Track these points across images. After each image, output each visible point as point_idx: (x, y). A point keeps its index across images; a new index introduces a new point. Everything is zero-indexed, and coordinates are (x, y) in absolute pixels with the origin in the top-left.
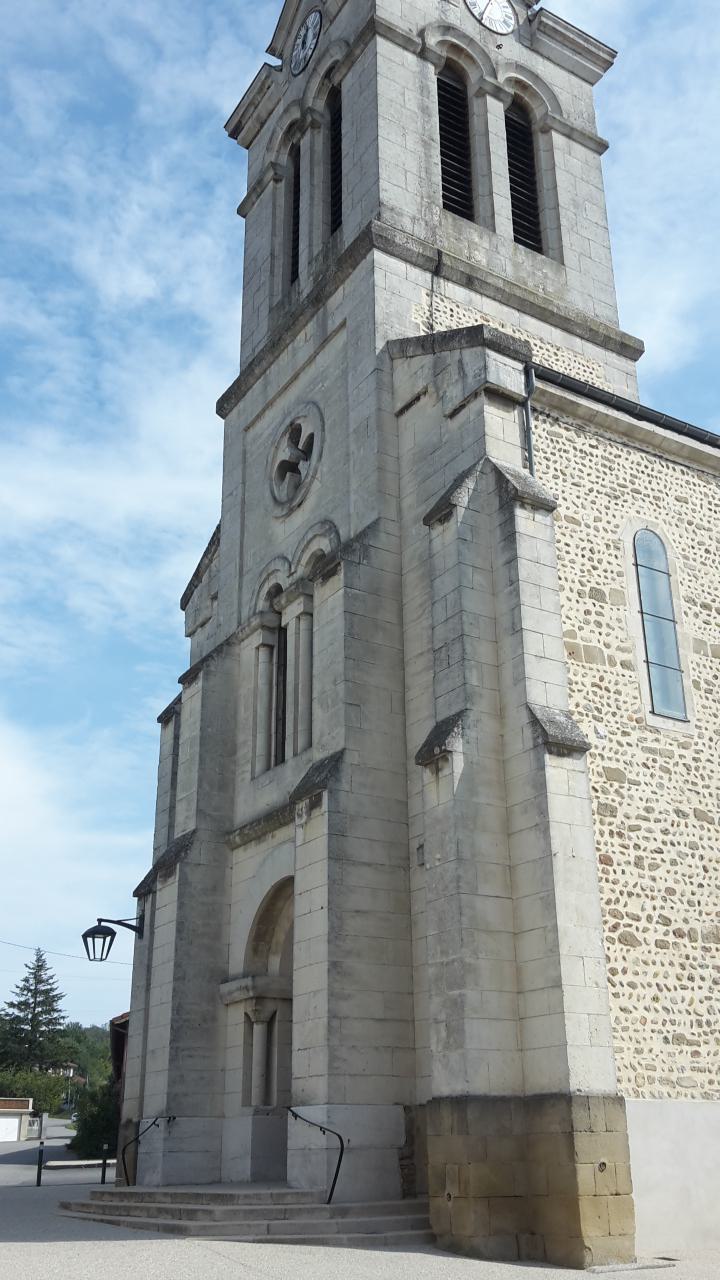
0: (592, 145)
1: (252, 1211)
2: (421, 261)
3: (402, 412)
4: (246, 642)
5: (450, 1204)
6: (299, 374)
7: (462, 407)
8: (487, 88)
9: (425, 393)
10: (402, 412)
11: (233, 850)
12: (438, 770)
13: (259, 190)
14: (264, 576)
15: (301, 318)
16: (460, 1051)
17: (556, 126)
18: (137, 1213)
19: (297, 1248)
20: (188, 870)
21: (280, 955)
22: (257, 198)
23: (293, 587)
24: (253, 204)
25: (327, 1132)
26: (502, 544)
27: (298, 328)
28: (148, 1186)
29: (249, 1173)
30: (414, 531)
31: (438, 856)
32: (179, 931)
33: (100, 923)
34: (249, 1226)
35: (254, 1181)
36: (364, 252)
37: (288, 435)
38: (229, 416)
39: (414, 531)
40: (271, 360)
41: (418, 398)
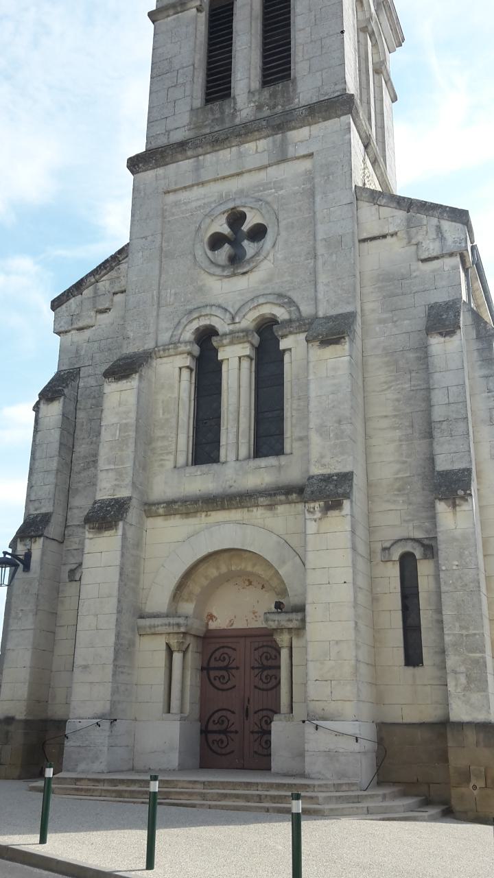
0: (392, 96)
1: (340, 797)
2: (364, 136)
3: (364, 240)
4: (165, 359)
5: (475, 792)
6: (243, 173)
7: (436, 258)
8: (370, 28)
9: (392, 235)
10: (364, 240)
11: (147, 517)
12: (454, 506)
13: (179, 9)
14: (195, 315)
15: (256, 133)
16: (483, 693)
17: (385, 73)
18: (126, 795)
19: (403, 823)
20: (126, 527)
21: (194, 603)
22: (175, 14)
23: (241, 334)
24: (168, 16)
25: (359, 740)
26: (480, 363)
27: (248, 139)
28: (278, 774)
29: (177, 764)
30: (377, 329)
31: (456, 563)
32: (121, 574)
33: (5, 556)
34: (357, 808)
35: (179, 770)
36: (339, 113)
37: (226, 215)
38: (140, 175)
39: (377, 329)
40: (208, 151)
41: (384, 236)
